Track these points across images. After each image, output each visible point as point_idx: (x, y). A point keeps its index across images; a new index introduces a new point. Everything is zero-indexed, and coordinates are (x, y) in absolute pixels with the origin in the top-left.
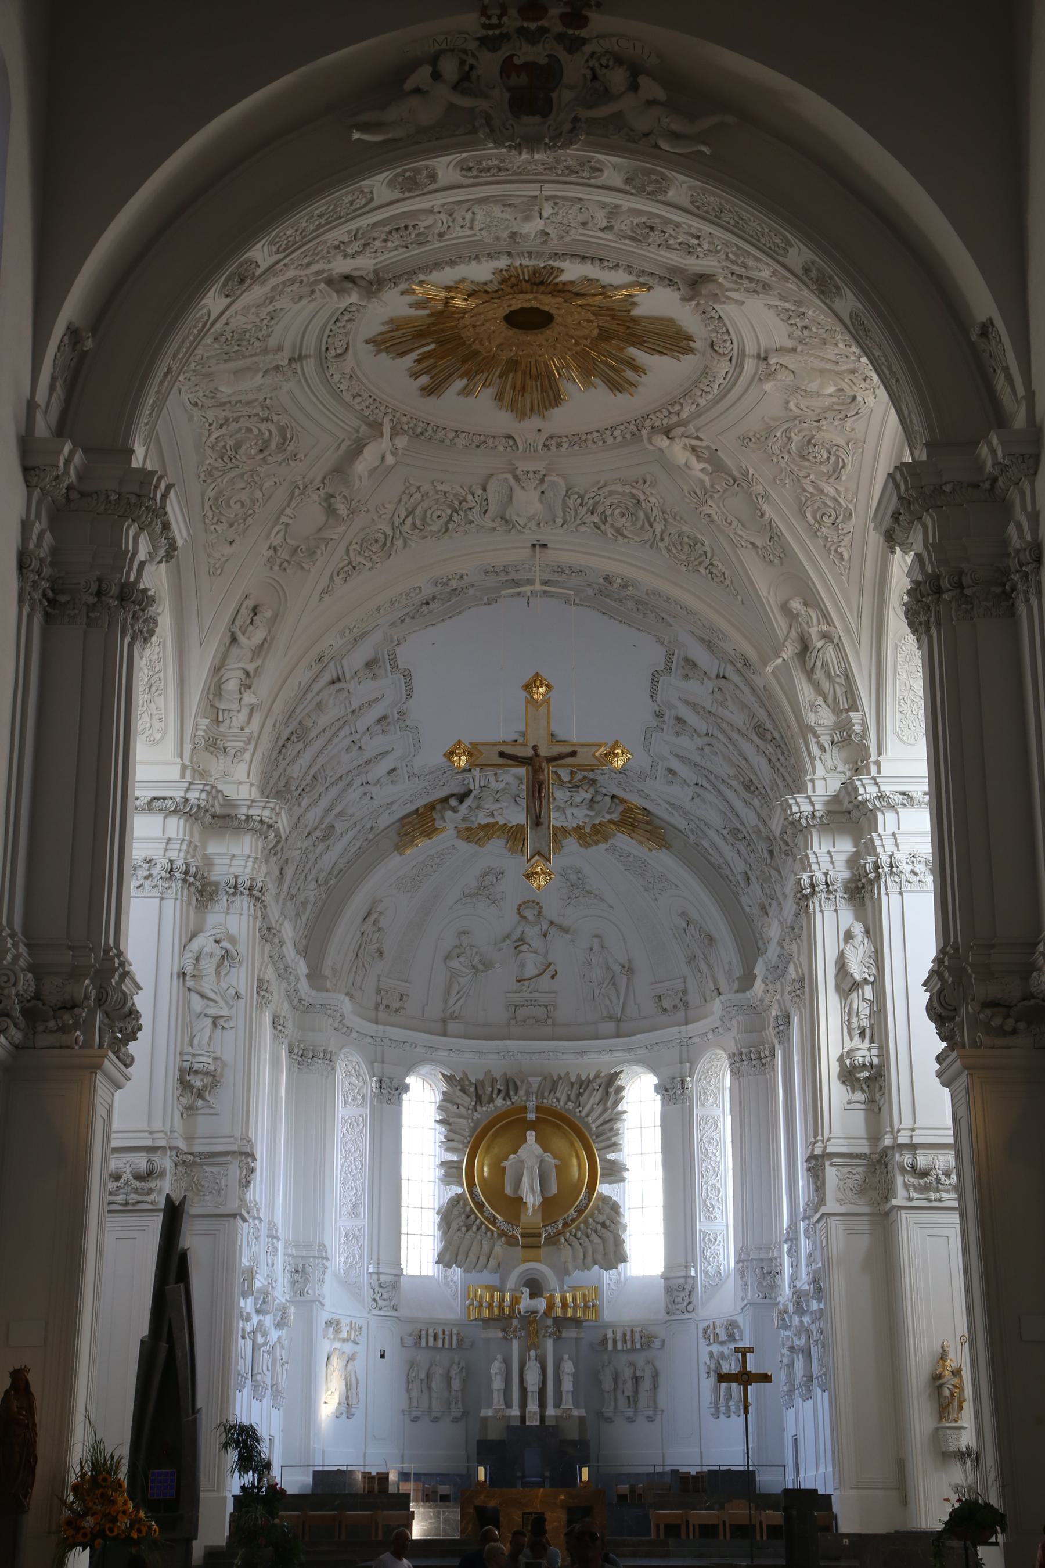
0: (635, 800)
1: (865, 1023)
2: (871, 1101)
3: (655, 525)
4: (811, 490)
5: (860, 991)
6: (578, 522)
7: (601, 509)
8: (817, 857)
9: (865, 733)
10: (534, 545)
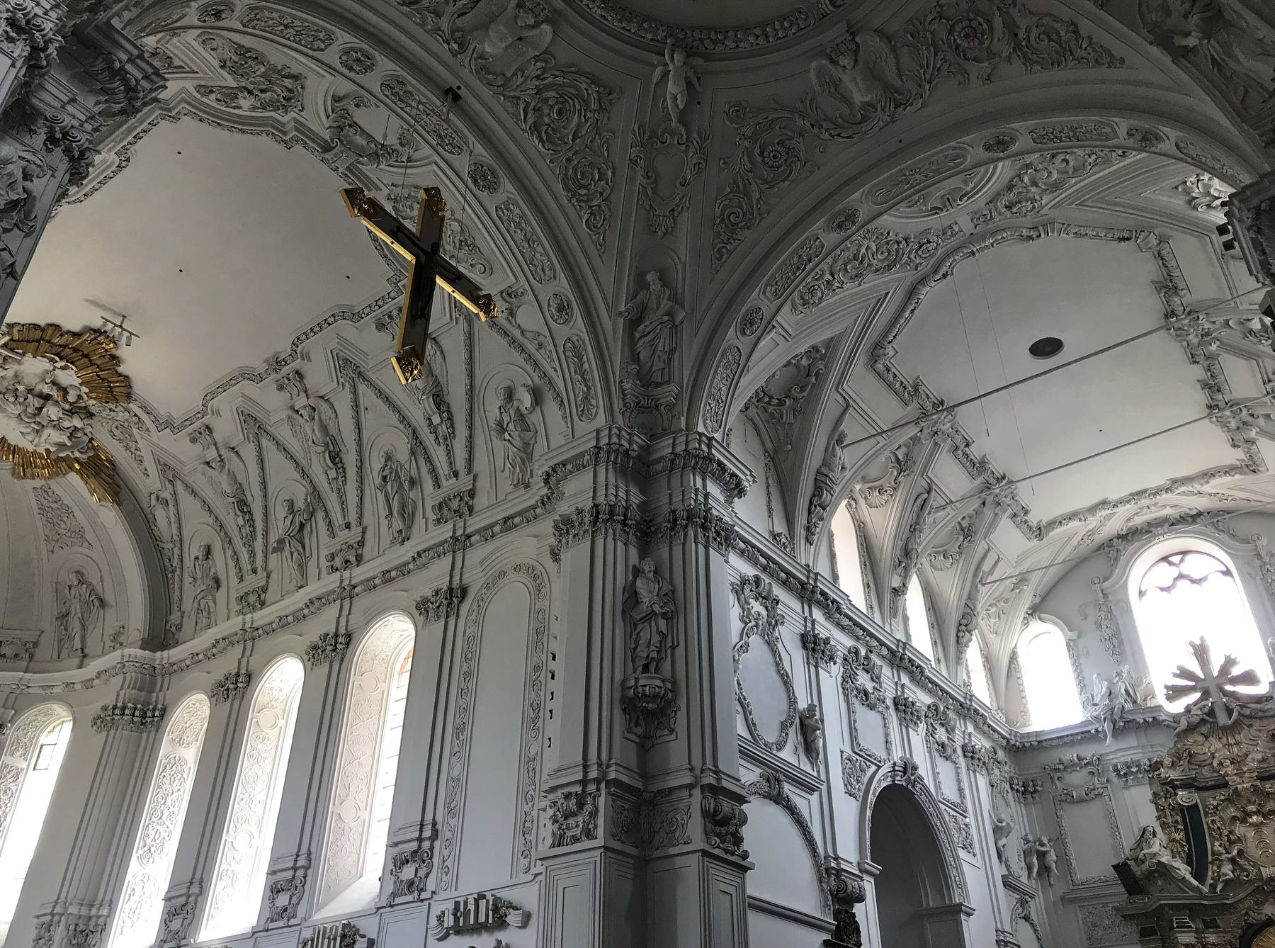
0: (114, 449)
1: (654, 655)
2: (645, 737)
3: (578, 141)
4: (741, 186)
5: (653, 624)
6: (517, 93)
7: (546, 95)
8: (617, 491)
9: (670, 407)
10: (451, 89)
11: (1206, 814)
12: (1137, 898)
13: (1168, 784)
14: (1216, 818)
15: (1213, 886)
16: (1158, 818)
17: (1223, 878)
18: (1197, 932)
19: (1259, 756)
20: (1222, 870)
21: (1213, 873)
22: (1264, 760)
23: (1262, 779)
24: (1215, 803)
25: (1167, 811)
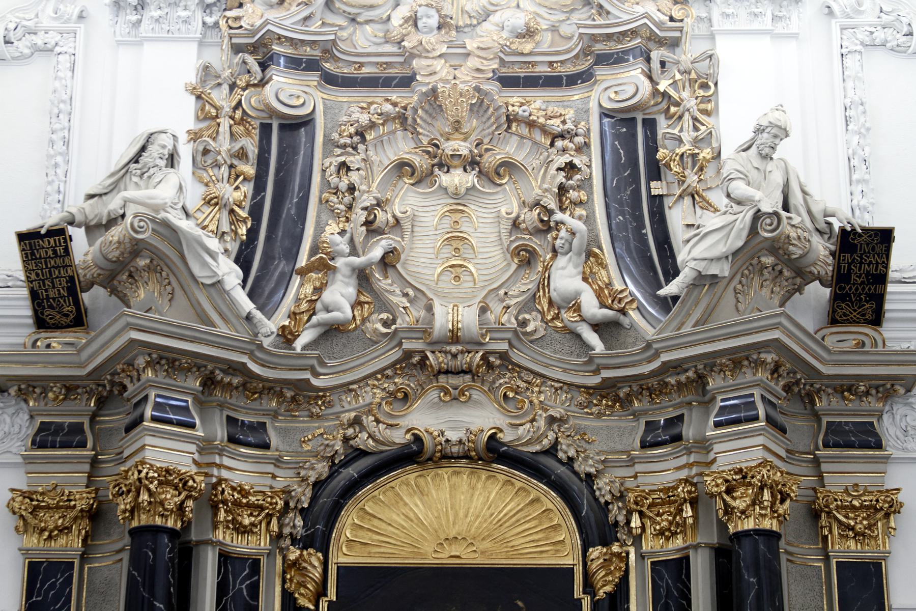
11: (329, 143)
12: (58, 341)
13: (253, 49)
14: (354, 160)
15: (287, 336)
16: (195, 136)
17: (321, 316)
18: (206, 447)
19: (519, 20)
20: (328, 296)
21: (298, 300)
22: (529, 33)
23: (509, 82)
24: (364, 119)
25: (225, 123)
